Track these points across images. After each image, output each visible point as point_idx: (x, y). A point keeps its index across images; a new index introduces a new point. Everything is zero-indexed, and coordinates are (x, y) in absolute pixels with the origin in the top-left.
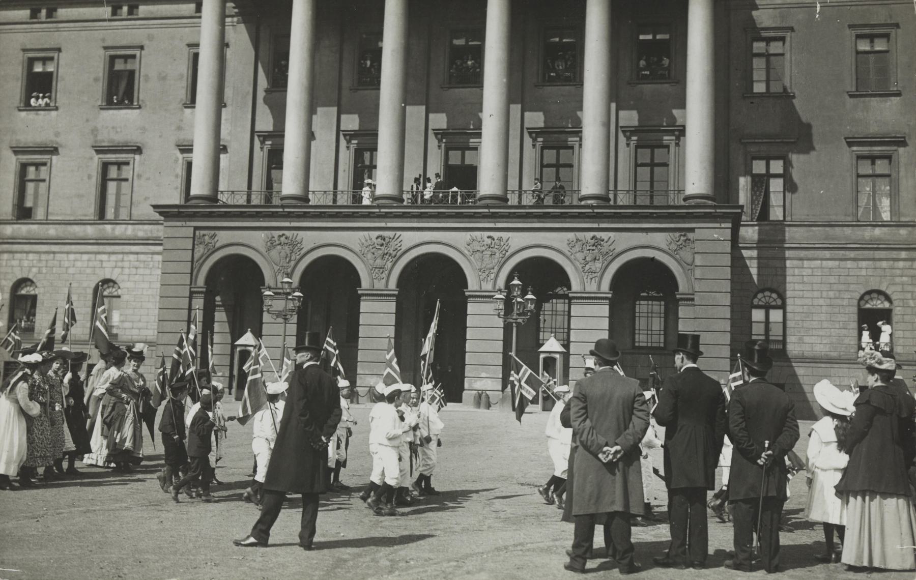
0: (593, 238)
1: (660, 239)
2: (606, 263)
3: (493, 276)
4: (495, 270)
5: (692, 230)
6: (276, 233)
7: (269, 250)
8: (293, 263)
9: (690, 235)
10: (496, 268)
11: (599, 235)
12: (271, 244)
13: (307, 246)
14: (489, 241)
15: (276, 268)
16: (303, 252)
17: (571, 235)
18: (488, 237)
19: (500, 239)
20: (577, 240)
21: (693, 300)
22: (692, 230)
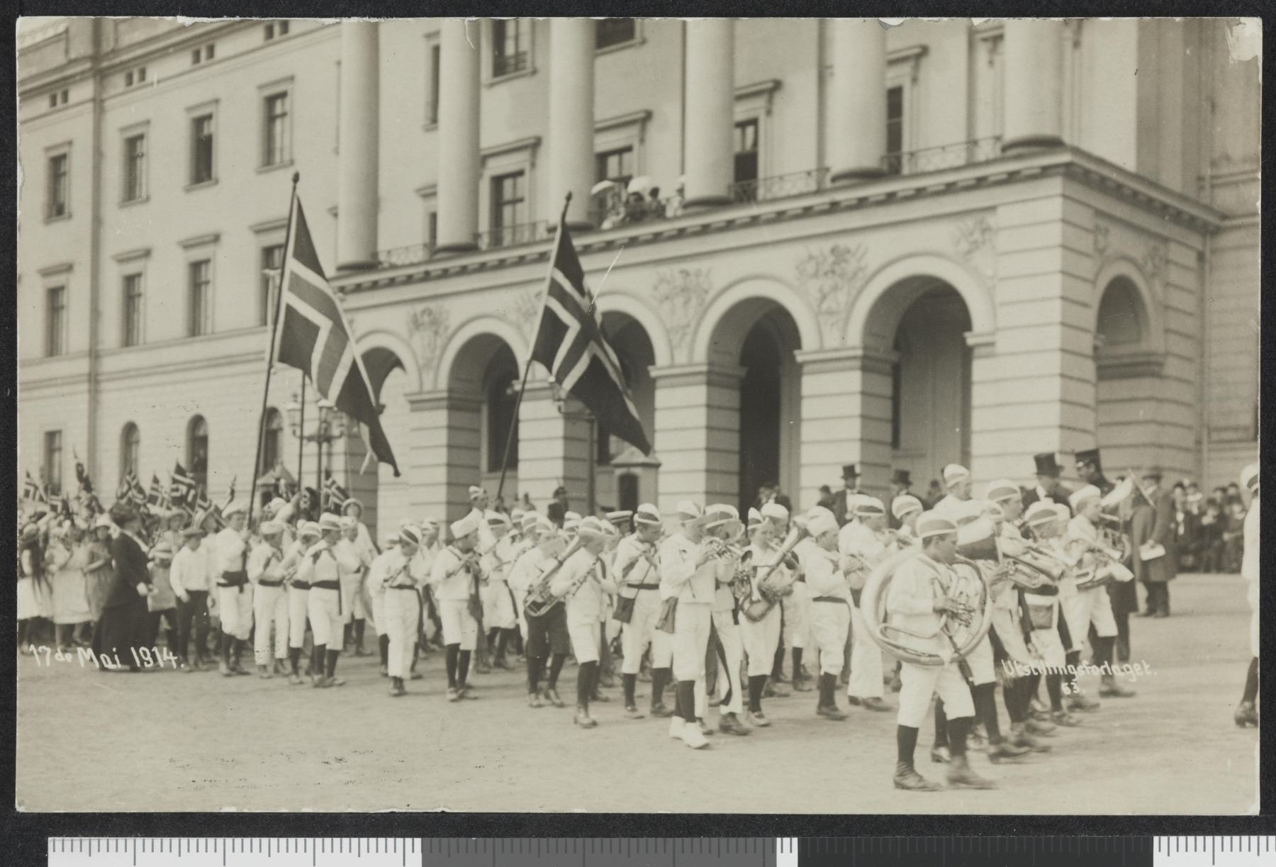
0: (833, 251)
1: (941, 236)
2: (854, 292)
3: (688, 338)
4: (690, 330)
5: (992, 209)
6: (419, 307)
7: (411, 334)
8: (438, 352)
9: (991, 220)
10: (693, 324)
11: (843, 242)
12: (416, 324)
13: (453, 322)
14: (679, 281)
15: (421, 362)
16: (450, 331)
17: (800, 250)
18: (682, 272)
19: (698, 274)
20: (811, 258)
21: (992, 344)
22: (992, 209)
